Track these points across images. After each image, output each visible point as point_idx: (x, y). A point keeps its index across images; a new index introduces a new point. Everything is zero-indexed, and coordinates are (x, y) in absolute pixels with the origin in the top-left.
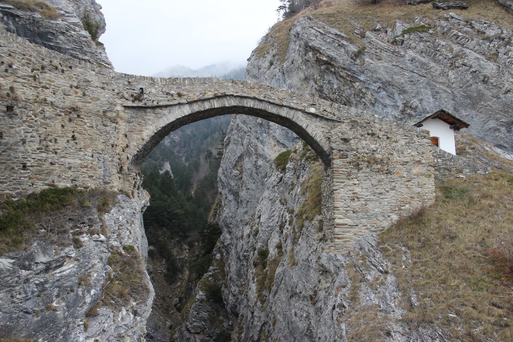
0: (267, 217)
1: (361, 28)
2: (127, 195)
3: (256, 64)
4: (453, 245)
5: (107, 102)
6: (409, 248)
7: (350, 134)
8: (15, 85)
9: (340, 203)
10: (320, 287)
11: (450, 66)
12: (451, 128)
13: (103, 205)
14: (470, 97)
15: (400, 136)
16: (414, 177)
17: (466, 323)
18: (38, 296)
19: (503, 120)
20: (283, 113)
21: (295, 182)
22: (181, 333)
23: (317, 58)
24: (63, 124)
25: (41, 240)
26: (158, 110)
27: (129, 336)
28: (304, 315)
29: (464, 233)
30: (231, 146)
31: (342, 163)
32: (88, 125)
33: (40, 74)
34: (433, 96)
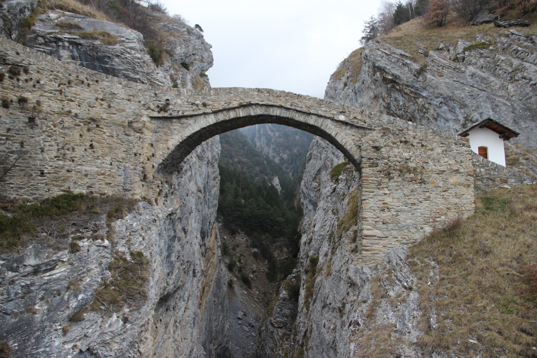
0: (320, 226)
1: (424, 48)
2: (150, 203)
3: (333, 86)
4: (486, 261)
5: (132, 113)
6: (439, 263)
7: (381, 142)
8: (42, 99)
9: (369, 213)
10: (348, 299)
11: (510, 80)
12: (500, 137)
13: (116, 211)
15: (436, 144)
16: (451, 186)
17: (487, 351)
18: (22, 298)
20: (311, 121)
21: (346, 193)
22: (266, 327)
23: (384, 77)
24: (82, 133)
25: (38, 243)
26: (184, 120)
27: (117, 343)
28: (332, 327)
29: (500, 248)
30: (312, 161)
31: (371, 172)
32: (108, 134)
33: (66, 88)
34: (493, 110)
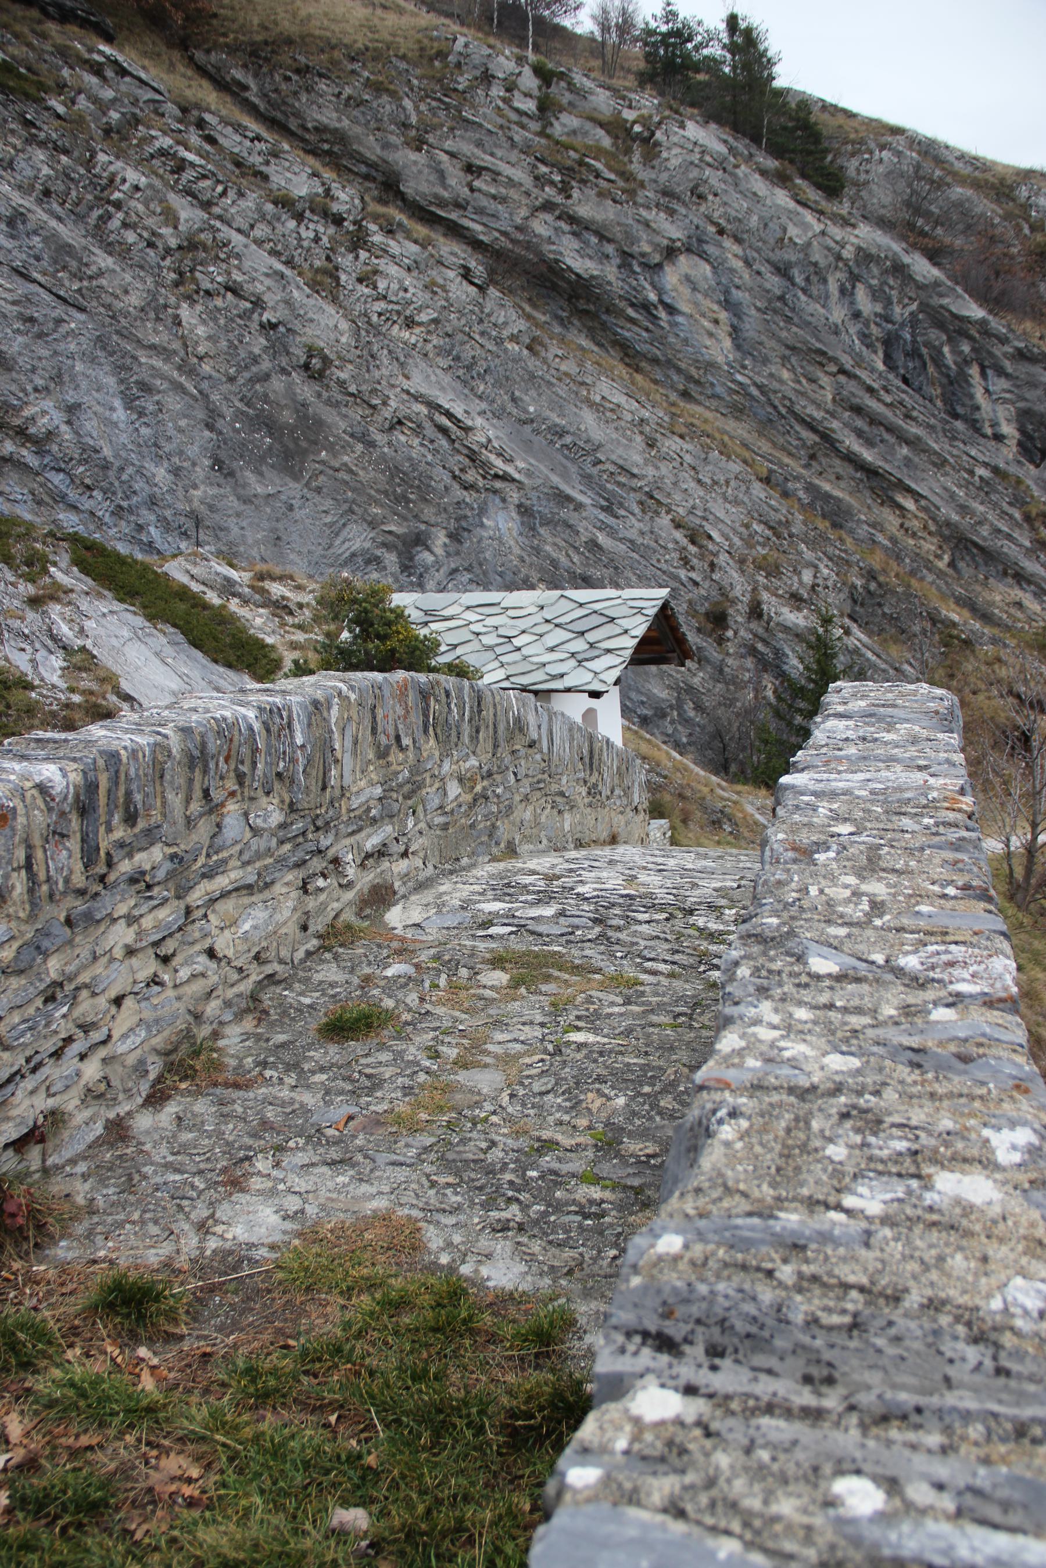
11: (177, 284)
14: (268, 424)
19: (393, 528)
34: (129, 403)
